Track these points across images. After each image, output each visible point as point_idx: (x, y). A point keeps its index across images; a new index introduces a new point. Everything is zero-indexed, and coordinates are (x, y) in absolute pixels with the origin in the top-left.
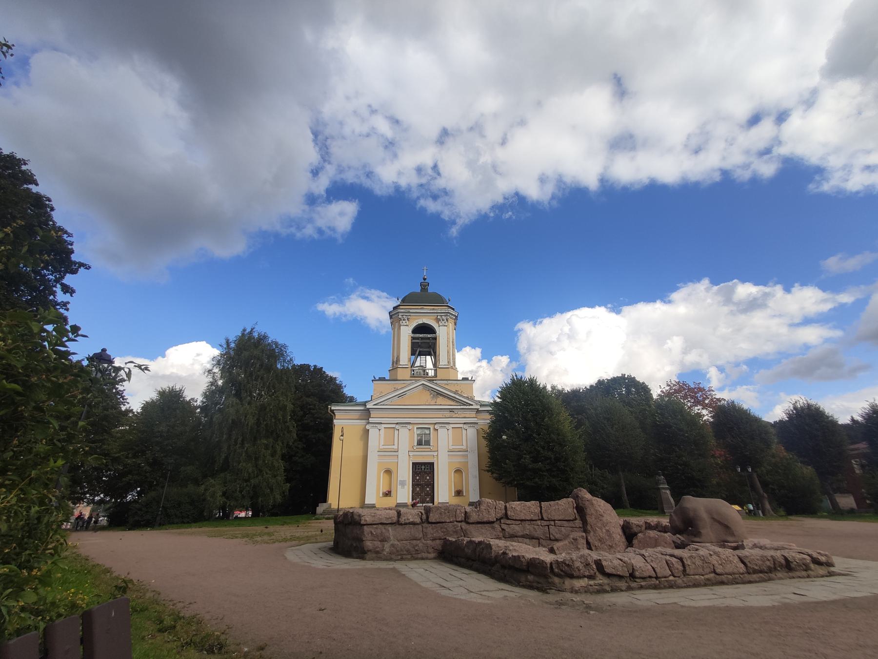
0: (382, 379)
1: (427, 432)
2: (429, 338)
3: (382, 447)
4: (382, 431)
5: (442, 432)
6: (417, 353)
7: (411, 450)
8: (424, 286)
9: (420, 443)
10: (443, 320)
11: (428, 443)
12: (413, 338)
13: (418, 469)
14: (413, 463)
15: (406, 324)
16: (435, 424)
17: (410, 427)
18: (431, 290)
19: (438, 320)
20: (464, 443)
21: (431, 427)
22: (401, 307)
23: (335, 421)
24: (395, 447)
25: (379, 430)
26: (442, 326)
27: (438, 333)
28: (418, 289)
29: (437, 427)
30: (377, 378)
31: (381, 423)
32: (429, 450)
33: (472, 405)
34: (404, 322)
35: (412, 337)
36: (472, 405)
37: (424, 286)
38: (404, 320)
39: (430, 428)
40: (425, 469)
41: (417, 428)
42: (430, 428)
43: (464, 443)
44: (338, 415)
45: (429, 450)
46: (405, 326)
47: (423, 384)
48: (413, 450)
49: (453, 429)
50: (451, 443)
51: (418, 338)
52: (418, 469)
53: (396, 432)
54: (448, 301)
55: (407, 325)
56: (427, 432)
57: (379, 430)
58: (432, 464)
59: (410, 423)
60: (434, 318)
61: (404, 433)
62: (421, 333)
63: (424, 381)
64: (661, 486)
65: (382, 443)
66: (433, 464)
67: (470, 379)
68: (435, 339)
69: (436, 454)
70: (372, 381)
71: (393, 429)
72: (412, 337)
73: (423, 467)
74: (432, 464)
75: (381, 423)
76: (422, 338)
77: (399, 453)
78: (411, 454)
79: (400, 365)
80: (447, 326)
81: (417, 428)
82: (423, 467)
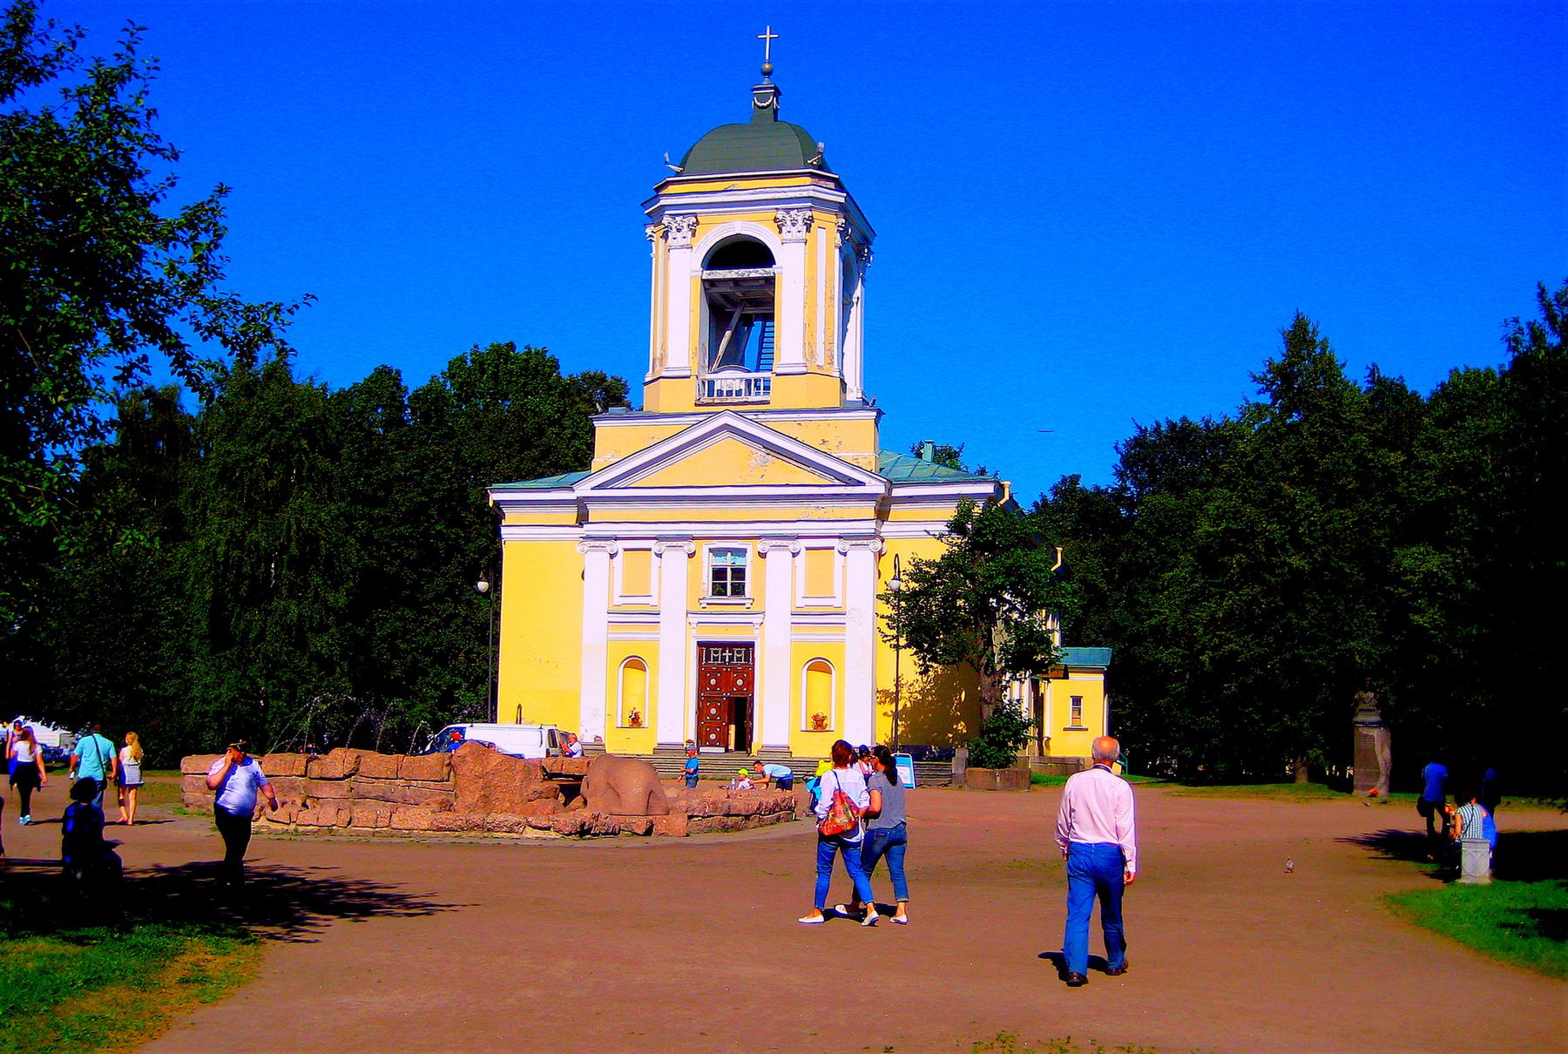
5: (779, 559)
7: (690, 610)
9: (719, 590)
11: (738, 590)
12: (709, 285)
13: (716, 659)
14: (700, 644)
15: (684, 242)
17: (691, 546)
20: (838, 592)
21: (749, 546)
22: (671, 189)
23: (503, 530)
26: (791, 241)
29: (761, 546)
31: (616, 539)
33: (861, 484)
35: (704, 281)
36: (861, 484)
38: (679, 230)
40: (731, 658)
42: (745, 550)
44: (511, 516)
46: (682, 247)
52: (716, 659)
56: (739, 562)
58: (749, 646)
60: (772, 215)
61: (675, 558)
63: (729, 416)
64: (1360, 718)
65: (618, 591)
68: (770, 281)
69: (756, 619)
72: (704, 281)
73: (727, 654)
74: (749, 646)
76: (736, 281)
78: (694, 619)
79: (667, 369)
81: (711, 550)
82: (727, 654)
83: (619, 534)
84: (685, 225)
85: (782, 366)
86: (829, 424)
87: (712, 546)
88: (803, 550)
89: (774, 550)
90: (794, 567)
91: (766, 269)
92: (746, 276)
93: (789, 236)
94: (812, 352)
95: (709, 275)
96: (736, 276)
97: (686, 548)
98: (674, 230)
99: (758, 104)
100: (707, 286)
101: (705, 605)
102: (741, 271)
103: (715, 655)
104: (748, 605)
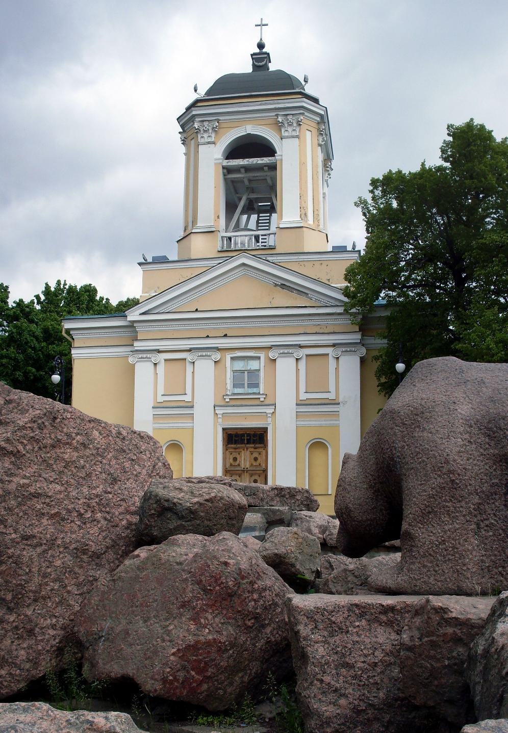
0: (161, 260)
1: (253, 365)
2: (260, 168)
3: (160, 399)
4: (161, 368)
6: (242, 204)
8: (261, 59)
10: (290, 125)
12: (228, 170)
14: (224, 429)
15: (209, 140)
16: (270, 348)
17: (217, 356)
18: (272, 67)
19: (279, 126)
20: (332, 388)
21: (262, 356)
22: (199, 104)
24: (188, 398)
25: (155, 364)
27: (278, 153)
28: (246, 67)
29: (272, 354)
30: (150, 260)
31: (159, 351)
32: (257, 402)
34: (205, 135)
35: (224, 168)
37: (261, 59)
38: (205, 131)
39: (259, 358)
41: (232, 358)
42: (259, 358)
43: (332, 388)
45: (257, 402)
46: (209, 143)
47: (244, 265)
48: (223, 404)
49: (308, 357)
50: (302, 388)
51: (237, 170)
53: (189, 368)
54: (303, 83)
55: (214, 143)
56: (253, 365)
57: (155, 364)
59: (218, 349)
62: (243, 157)
63: (246, 257)
65: (161, 390)
66: (265, 430)
67: (349, 248)
68: (273, 168)
69: (270, 410)
70: (140, 264)
71: (181, 363)
72: (224, 168)
75: (159, 351)
76: (247, 169)
77: (196, 411)
78: (220, 411)
80: (297, 137)
81: (232, 358)
83: (161, 348)
84: (210, 128)
85: (285, 223)
86: (322, 264)
87: (232, 356)
88: (305, 357)
89: (281, 357)
90: (298, 370)
91: (270, 158)
92: (255, 162)
93: (286, 134)
94: (305, 214)
95: (228, 163)
96: (247, 163)
97: (213, 357)
98: (202, 132)
99: (256, 63)
100: (225, 171)
101: (227, 400)
102: (251, 160)
103: (255, 439)
104: (262, 399)
